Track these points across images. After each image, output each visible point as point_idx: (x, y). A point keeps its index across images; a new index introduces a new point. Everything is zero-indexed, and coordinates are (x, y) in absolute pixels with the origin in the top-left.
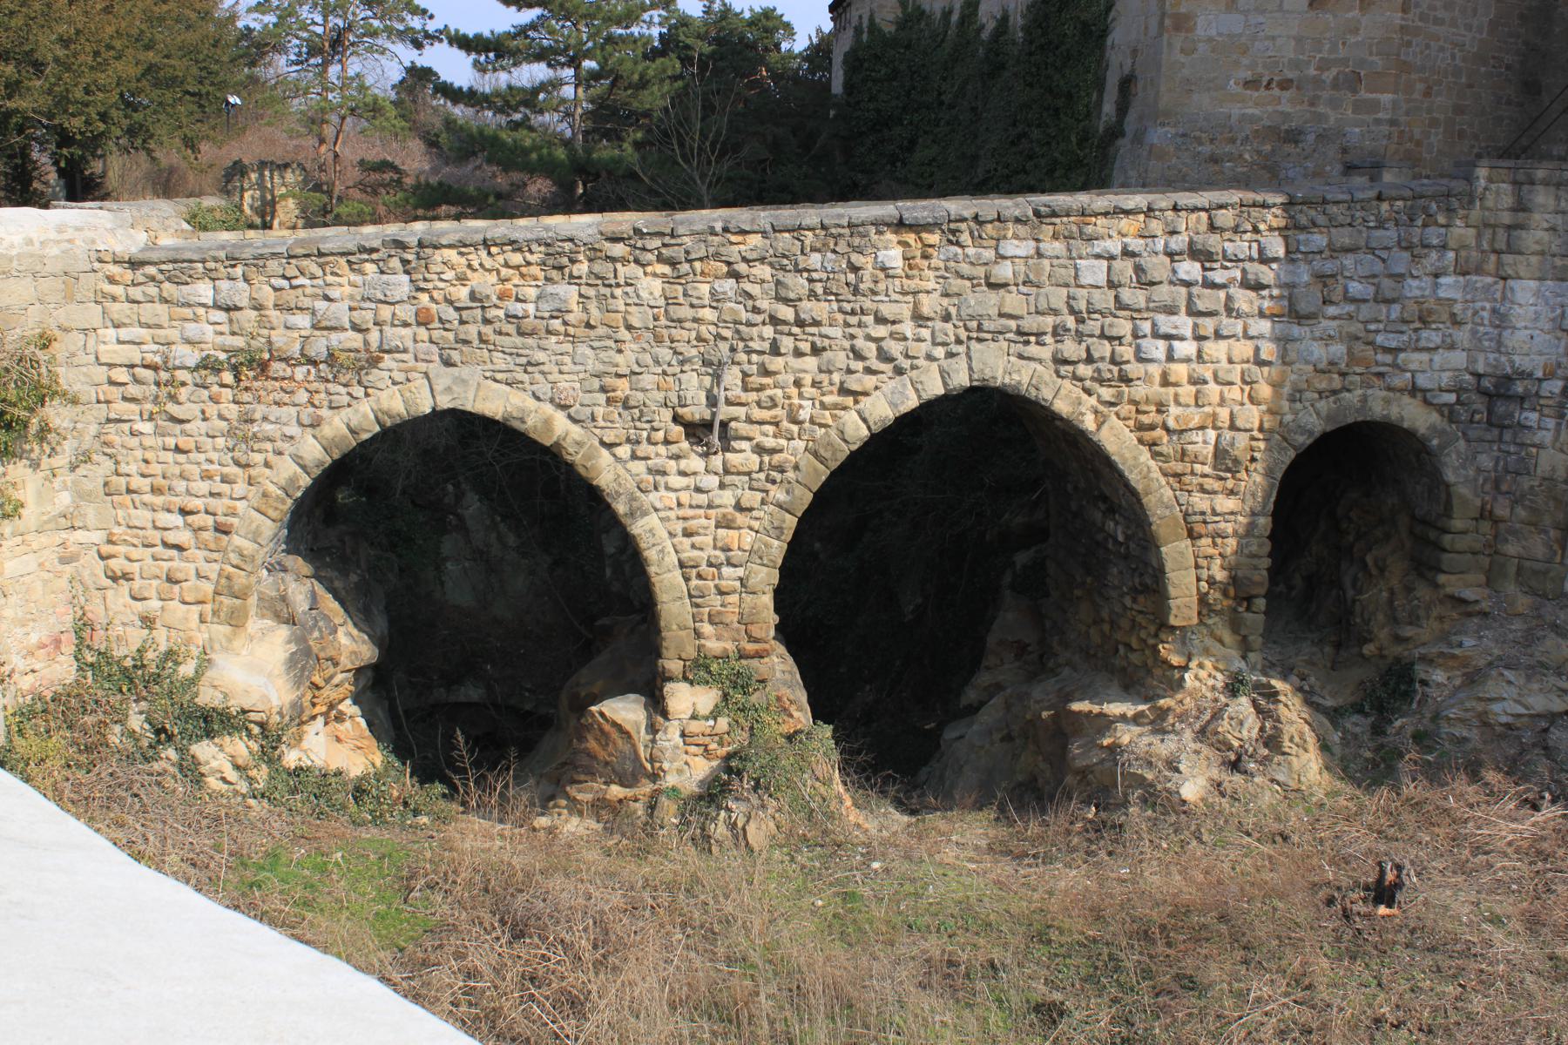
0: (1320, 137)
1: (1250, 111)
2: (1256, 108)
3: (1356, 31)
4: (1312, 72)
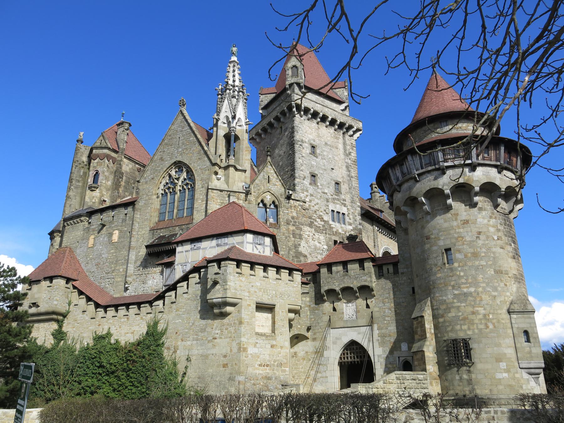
0: (276, 378)
1: (260, 372)
2: (261, 371)
3: (280, 353)
4: (272, 363)
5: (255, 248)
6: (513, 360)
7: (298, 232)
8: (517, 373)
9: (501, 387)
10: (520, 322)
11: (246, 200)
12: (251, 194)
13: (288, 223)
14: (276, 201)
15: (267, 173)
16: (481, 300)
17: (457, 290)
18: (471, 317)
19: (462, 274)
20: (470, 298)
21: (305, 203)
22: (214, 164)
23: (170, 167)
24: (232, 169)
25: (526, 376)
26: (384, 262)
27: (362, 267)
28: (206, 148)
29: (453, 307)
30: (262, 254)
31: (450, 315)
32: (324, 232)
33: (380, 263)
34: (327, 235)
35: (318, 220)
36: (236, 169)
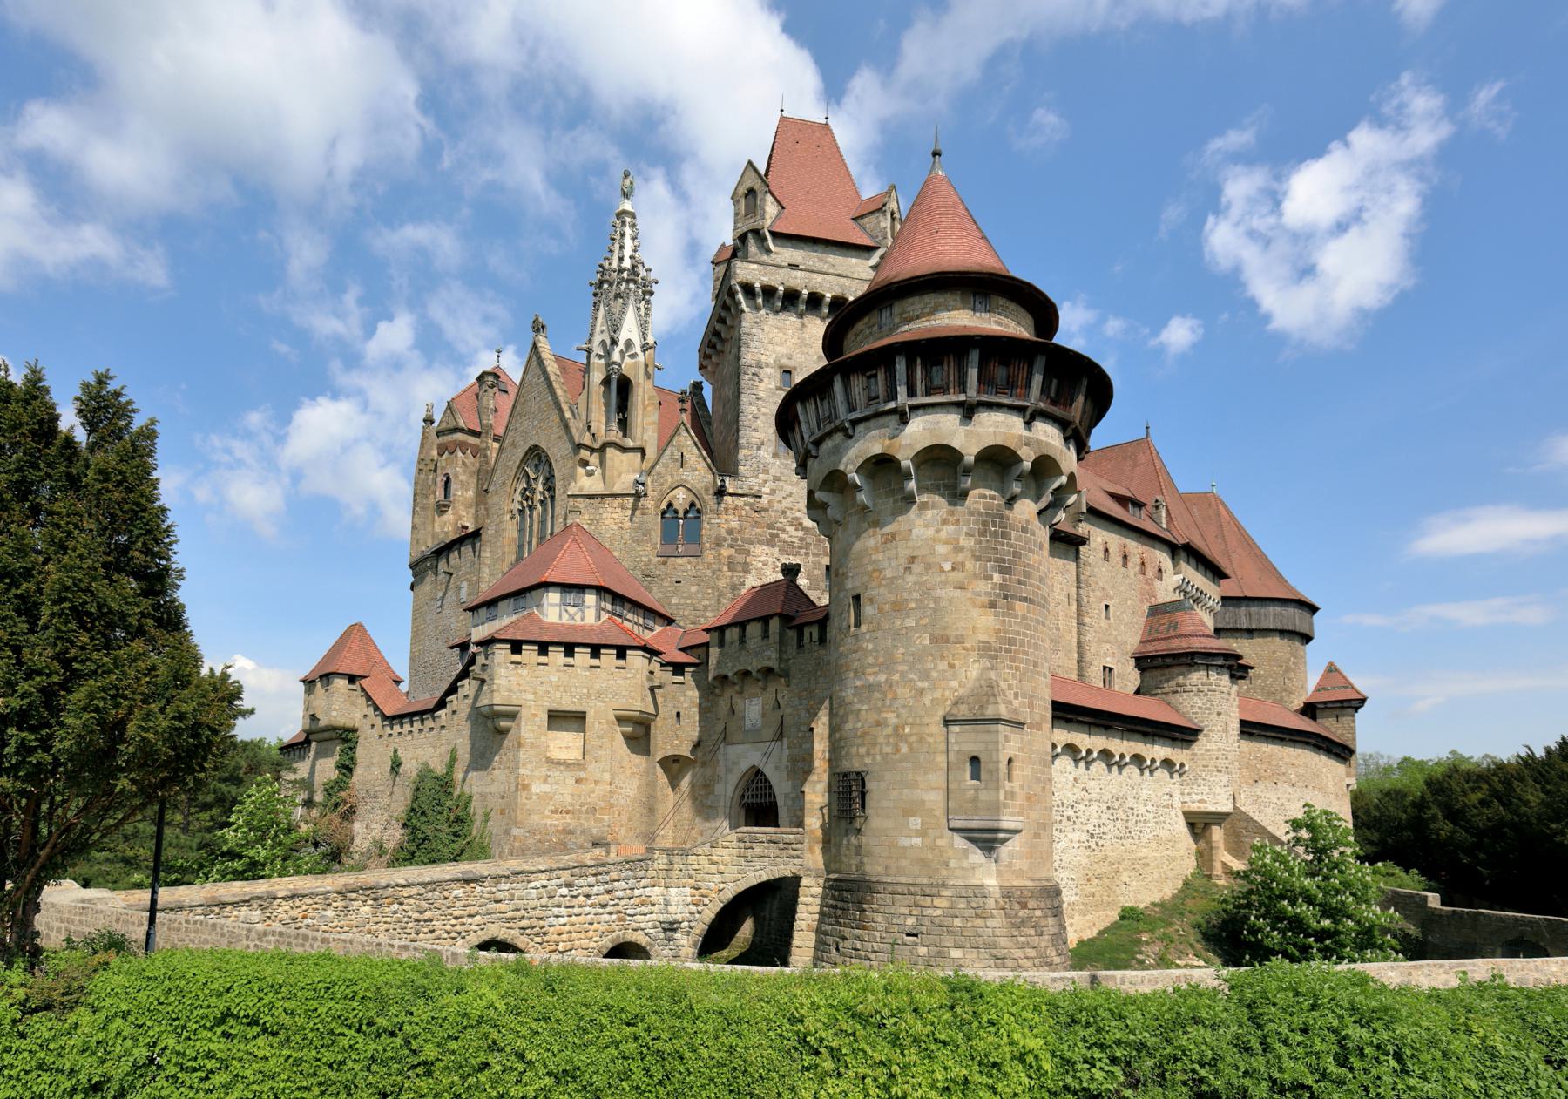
5: (564, 613)
6: (937, 813)
7: (740, 558)
8: (942, 837)
9: (904, 863)
10: (966, 740)
11: (635, 508)
12: (646, 495)
13: (718, 544)
14: (697, 502)
15: (679, 447)
16: (895, 698)
17: (860, 679)
18: (874, 731)
19: (870, 646)
20: (877, 695)
21: (760, 497)
22: (580, 446)
23: (524, 460)
24: (610, 451)
25: (960, 842)
26: (805, 620)
27: (765, 635)
28: (568, 415)
29: (852, 711)
30: (579, 622)
31: (848, 726)
32: (803, 551)
33: (796, 622)
34: (811, 558)
35: (788, 528)
36: (624, 449)
